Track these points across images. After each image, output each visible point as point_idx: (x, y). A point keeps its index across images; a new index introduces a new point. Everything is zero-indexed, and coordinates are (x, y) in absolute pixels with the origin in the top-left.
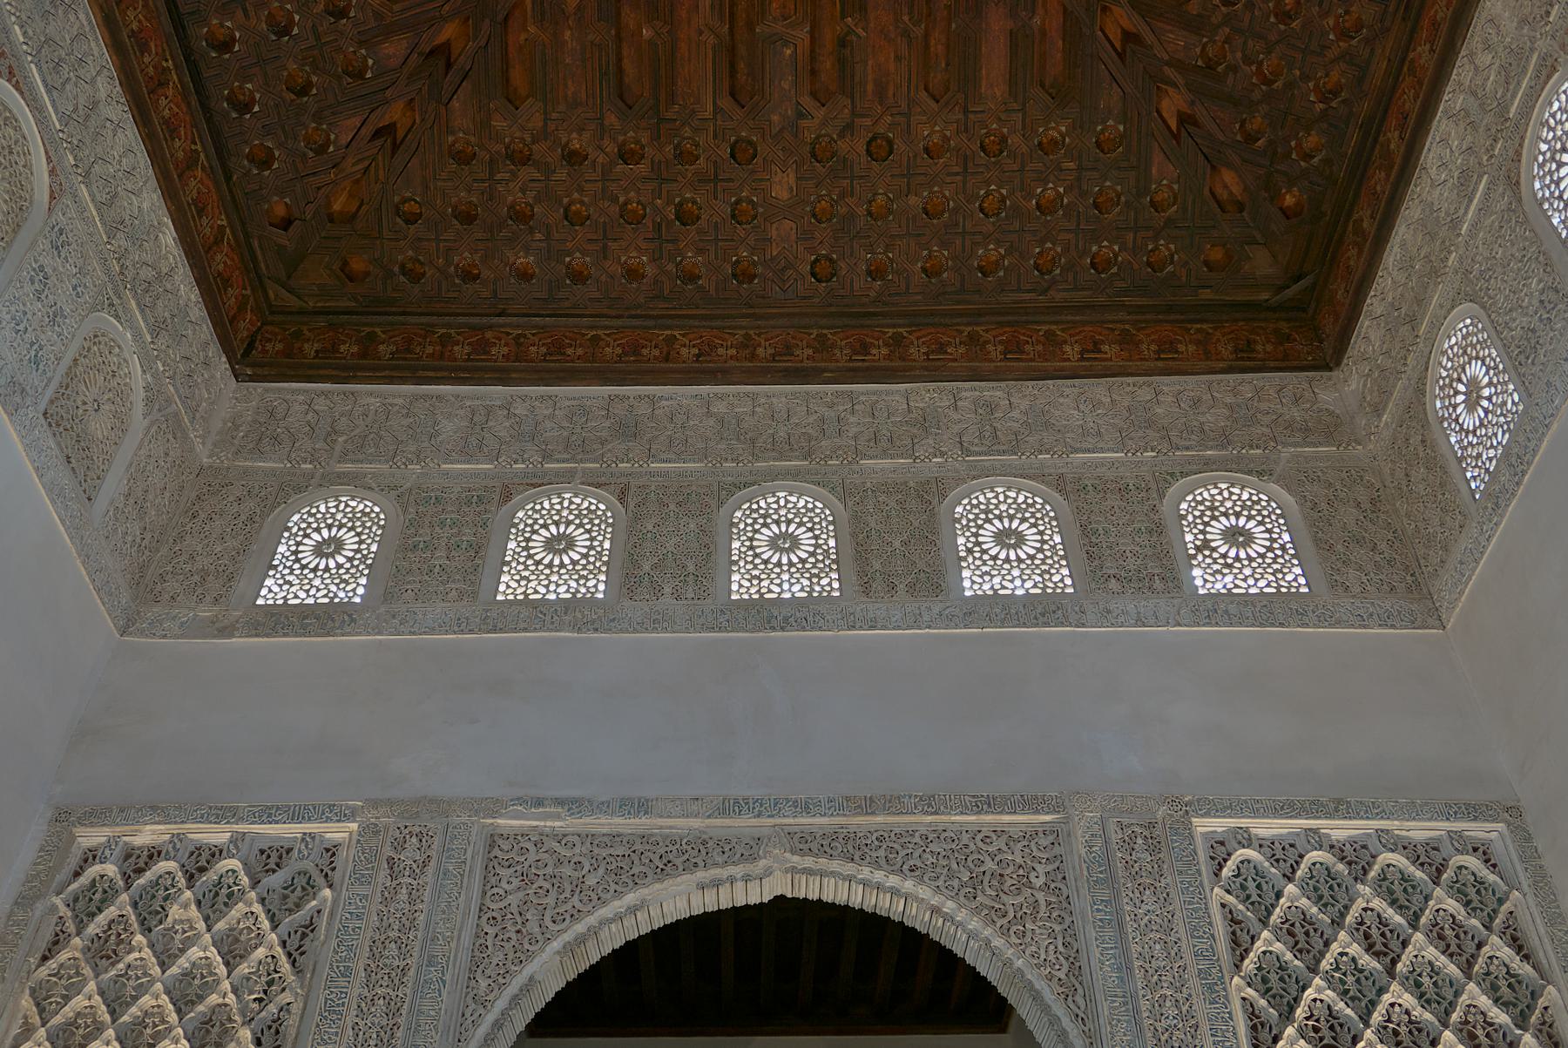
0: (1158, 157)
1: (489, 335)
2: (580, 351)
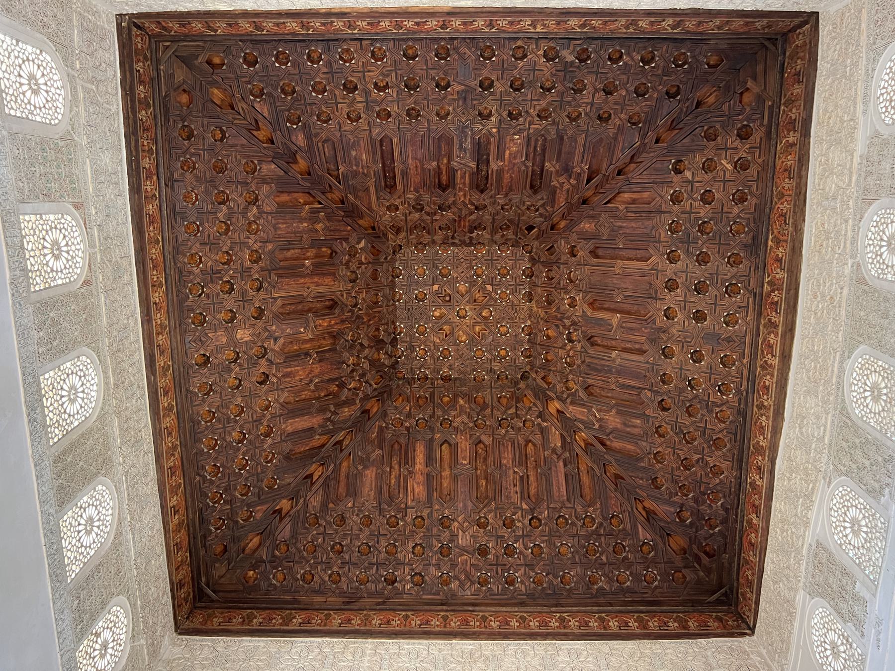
0: (264, 507)
1: (155, 178)
2: (152, 234)
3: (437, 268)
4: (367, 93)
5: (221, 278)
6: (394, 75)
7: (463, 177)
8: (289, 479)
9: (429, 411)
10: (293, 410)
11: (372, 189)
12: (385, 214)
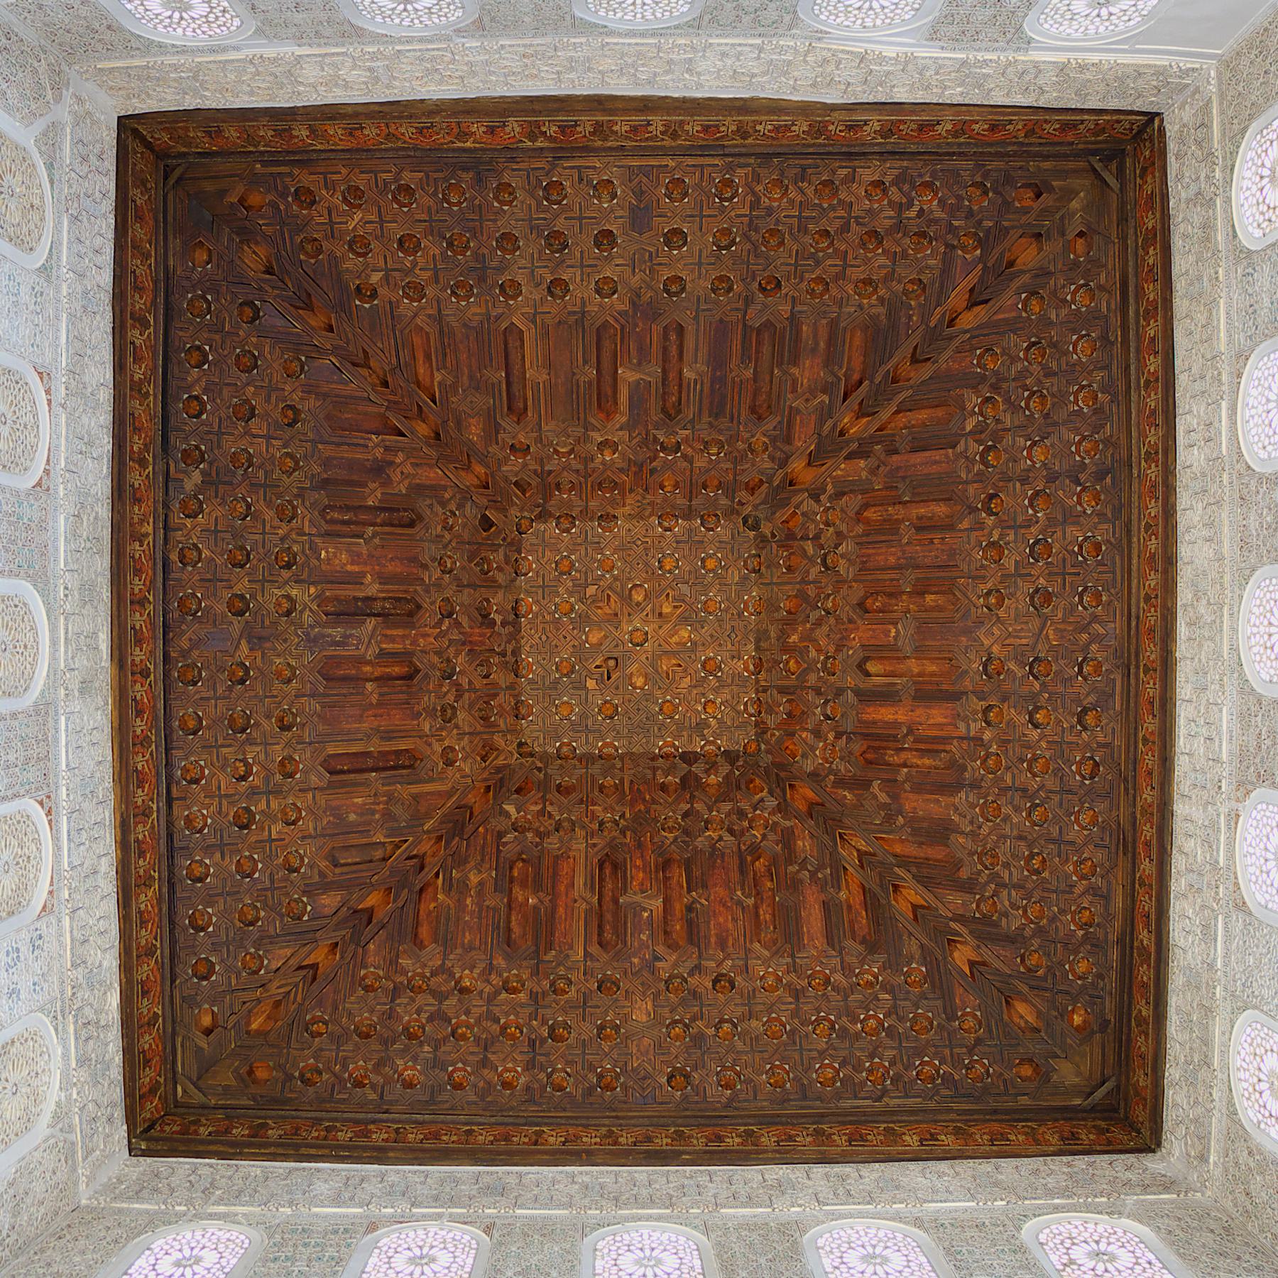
1: (372, 1127)
2: (454, 1138)
3: (557, 682)
4: (254, 792)
5: (543, 1041)
6: (224, 750)
7: (392, 639)
8: (911, 947)
9: (811, 696)
10: (789, 933)
11: (415, 789)
12: (460, 769)
